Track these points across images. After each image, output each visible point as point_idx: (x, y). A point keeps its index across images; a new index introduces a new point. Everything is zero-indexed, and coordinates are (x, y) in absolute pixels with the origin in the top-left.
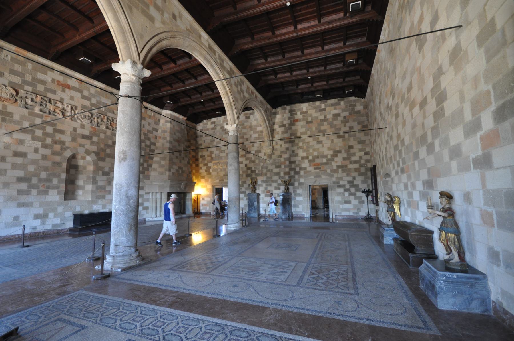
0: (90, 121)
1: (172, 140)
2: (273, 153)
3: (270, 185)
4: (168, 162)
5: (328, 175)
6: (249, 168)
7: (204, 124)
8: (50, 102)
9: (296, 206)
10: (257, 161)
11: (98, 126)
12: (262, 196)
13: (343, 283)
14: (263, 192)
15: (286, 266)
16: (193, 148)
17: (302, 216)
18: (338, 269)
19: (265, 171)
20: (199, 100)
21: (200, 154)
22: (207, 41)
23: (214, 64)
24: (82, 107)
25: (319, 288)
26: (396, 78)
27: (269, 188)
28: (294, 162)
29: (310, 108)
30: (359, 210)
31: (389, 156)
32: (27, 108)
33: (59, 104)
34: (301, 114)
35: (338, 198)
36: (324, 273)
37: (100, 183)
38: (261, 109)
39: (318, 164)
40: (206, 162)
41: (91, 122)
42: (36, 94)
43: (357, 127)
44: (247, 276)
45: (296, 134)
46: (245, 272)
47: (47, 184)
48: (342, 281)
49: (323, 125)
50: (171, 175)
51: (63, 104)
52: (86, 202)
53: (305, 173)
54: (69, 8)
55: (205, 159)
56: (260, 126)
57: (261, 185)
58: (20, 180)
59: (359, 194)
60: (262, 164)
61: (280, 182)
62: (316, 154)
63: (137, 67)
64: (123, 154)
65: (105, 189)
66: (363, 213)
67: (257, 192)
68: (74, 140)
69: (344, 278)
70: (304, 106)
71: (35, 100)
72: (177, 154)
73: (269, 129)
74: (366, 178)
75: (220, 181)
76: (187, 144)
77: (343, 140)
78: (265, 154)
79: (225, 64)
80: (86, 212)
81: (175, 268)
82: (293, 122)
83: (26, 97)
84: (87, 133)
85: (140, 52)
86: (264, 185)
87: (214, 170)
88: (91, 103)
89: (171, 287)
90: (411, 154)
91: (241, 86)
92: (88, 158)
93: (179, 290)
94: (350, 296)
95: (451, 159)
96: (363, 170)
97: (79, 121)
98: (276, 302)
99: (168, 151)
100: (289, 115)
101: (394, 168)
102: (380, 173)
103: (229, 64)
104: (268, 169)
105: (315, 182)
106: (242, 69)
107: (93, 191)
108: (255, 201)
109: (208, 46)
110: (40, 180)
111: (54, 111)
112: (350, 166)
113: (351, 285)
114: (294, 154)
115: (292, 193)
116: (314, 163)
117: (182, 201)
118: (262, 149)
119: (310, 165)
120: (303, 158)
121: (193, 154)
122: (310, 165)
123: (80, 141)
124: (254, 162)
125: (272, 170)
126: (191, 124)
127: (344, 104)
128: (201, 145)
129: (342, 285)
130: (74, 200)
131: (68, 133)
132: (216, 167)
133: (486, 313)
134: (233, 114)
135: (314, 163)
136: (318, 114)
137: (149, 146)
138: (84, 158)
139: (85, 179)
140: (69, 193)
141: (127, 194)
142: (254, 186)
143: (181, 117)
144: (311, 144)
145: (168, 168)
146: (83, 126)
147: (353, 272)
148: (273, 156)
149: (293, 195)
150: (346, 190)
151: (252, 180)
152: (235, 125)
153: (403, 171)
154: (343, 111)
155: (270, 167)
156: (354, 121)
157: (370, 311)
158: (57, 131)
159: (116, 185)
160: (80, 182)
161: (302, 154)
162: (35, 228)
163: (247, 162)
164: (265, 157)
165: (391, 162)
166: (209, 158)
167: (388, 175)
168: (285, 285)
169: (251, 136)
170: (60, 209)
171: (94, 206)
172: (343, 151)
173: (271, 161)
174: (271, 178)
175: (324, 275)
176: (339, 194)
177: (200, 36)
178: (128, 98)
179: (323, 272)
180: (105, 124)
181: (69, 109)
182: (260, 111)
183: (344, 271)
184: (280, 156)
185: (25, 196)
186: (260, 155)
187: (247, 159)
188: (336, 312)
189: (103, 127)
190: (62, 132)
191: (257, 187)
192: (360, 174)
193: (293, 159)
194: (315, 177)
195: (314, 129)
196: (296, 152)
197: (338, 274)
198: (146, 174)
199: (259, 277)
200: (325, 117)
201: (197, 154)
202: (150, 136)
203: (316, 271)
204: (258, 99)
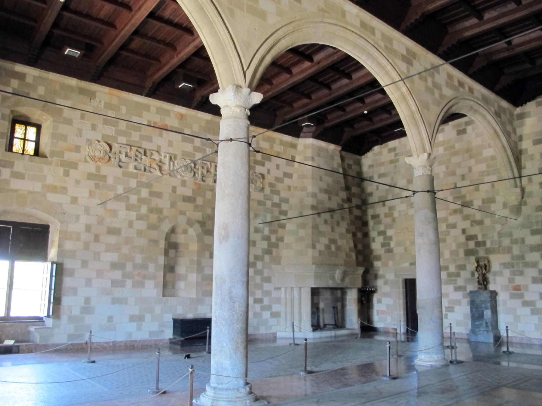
0: (193, 174)
1: (316, 190)
3: (521, 273)
4: (310, 231)
6: (469, 238)
7: (375, 155)
8: (145, 154)
10: (488, 222)
11: (203, 181)
16: (356, 201)
19: (506, 242)
20: (359, 112)
21: (370, 212)
22: (357, 16)
24: (183, 155)
27: (519, 280)
32: (120, 166)
33: (156, 156)
38: (485, 112)
40: (382, 228)
41: (194, 175)
42: (131, 146)
50: (317, 254)
51: (160, 154)
54: (163, 25)
55: (380, 222)
56: (490, 146)
57: (501, 274)
58: (114, 266)
60: (498, 227)
67: (492, 287)
68: (173, 205)
71: (129, 154)
72: (327, 216)
78: (505, 206)
83: (120, 152)
84: (189, 192)
85: (245, 69)
86: (507, 272)
87: (399, 244)
88: (194, 147)
91: (433, 76)
92: (191, 231)
97: (179, 176)
99: (311, 212)
103: (403, 42)
106: (431, 45)
107: (198, 284)
108: (486, 308)
109: (359, 25)
110: (135, 266)
111: (150, 167)
117: (339, 305)
121: (357, 212)
123: (182, 205)
124: (480, 223)
125: (523, 240)
126: (350, 158)
128: (371, 194)
130: (174, 296)
131: (166, 196)
134: (420, 133)
137: (277, 205)
138: (185, 232)
140: (168, 287)
141: (230, 293)
142: (484, 275)
143: (332, 147)
145: (310, 242)
146: (184, 183)
151: (478, 262)
152: (426, 155)
155: (518, 234)
159: (216, 278)
160: (181, 270)
162: (130, 334)
163: (466, 224)
164: (506, 212)
166: (388, 220)
169: (470, 169)
170: (158, 310)
171: (199, 307)
174: (522, 257)
177: (343, 13)
180: (213, 175)
181: (167, 160)
182: (484, 117)
185: (119, 289)
186: (493, 207)
187: (466, 218)
190: (159, 195)
191: (490, 276)
198: (274, 254)
201: (365, 212)
202: (280, 186)
204: (476, 94)
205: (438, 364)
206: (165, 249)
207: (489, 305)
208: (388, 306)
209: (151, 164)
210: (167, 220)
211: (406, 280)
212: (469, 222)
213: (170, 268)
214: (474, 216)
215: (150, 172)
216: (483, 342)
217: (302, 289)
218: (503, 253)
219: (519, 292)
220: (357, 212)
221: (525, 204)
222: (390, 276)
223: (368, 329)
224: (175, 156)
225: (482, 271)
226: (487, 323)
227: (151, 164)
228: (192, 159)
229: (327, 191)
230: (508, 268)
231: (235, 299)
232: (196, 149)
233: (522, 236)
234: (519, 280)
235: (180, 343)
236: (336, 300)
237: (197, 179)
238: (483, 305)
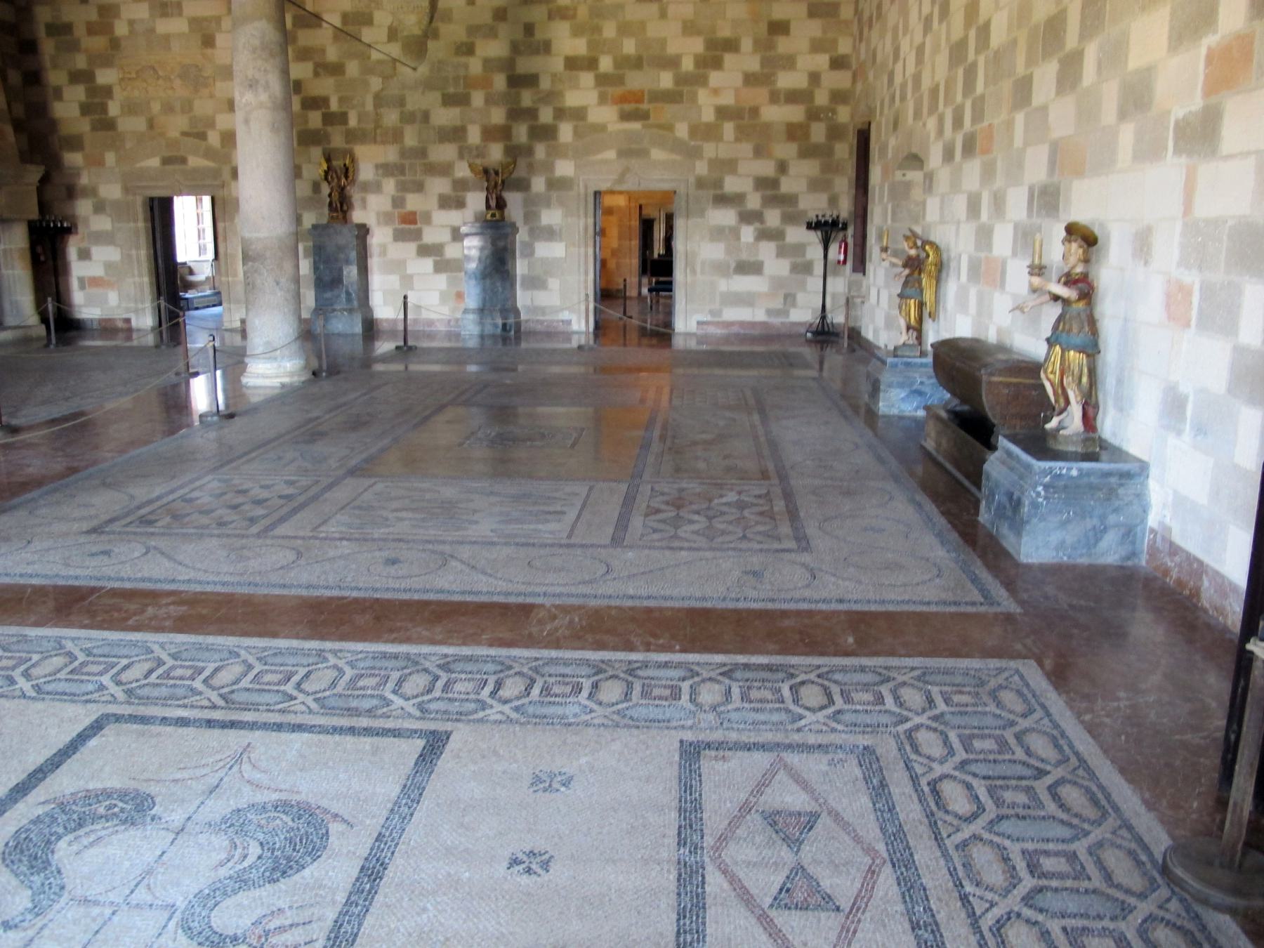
2: (430, 33)
3: (419, 187)
5: (678, 146)
6: (313, 103)
9: (535, 283)
10: (353, 69)
12: (380, 237)
13: (761, 528)
14: (386, 218)
15: (557, 495)
17: (561, 327)
18: (740, 493)
19: (391, 117)
25: (686, 545)
27: (413, 202)
28: (530, 80)
30: (790, 299)
31: (926, 83)
35: (712, 251)
36: (694, 507)
39: (637, 97)
40: (81, 62)
44: (422, 531)
48: (757, 523)
53: (576, 133)
55: (74, 47)
57: (377, 188)
59: (798, 234)
60: (376, 83)
66: (804, 314)
67: (358, 216)
69: (761, 514)
74: (830, 168)
75: (166, 161)
78: (393, 34)
81: (116, 527)
86: (390, 185)
87: (131, 109)
89: (143, 580)
90: (1006, 86)
93: (183, 587)
94: (787, 556)
95: (1123, 115)
96: (818, 133)
98: (558, 590)
101: (940, 132)
102: (883, 149)
104: (410, 107)
105: (621, 179)
108: (348, 262)
113: (785, 529)
115: (520, 224)
119: (603, 99)
120: (573, 64)
122: (603, 99)
124: (336, 69)
125: (426, 116)
129: (760, 533)
133: (1130, 563)
142: (343, 189)
147: (788, 496)
149: (522, 236)
150: (748, 217)
151: (328, 160)
153: (969, 148)
155: (416, 101)
157: (847, 583)
161: (567, 42)
164: (395, 50)
165: (933, 108)
166: (98, 43)
167: (915, 160)
168: (568, 546)
172: (747, 44)
173: (423, 69)
174: (422, 153)
175: (698, 513)
176: (718, 233)
179: (691, 503)
183: (760, 497)
184: (469, 50)
186: (367, 35)
188: (754, 594)
191: (355, 195)
192: (808, 152)
193: (525, 65)
194: (624, 153)
196: (539, 35)
197: (741, 506)
199: (470, 532)
203: (667, 503)
205: (296, 380)
207: (353, 255)
208: (108, 266)
211: (152, 199)
214: (323, 51)
216: (339, 335)
218: (383, 143)
219: (412, 227)
221: (436, 35)
222: (111, 191)
223: (63, 325)
225: (339, 179)
226: (348, 294)
230: (392, 175)
234: (413, 202)
238: (342, 256)
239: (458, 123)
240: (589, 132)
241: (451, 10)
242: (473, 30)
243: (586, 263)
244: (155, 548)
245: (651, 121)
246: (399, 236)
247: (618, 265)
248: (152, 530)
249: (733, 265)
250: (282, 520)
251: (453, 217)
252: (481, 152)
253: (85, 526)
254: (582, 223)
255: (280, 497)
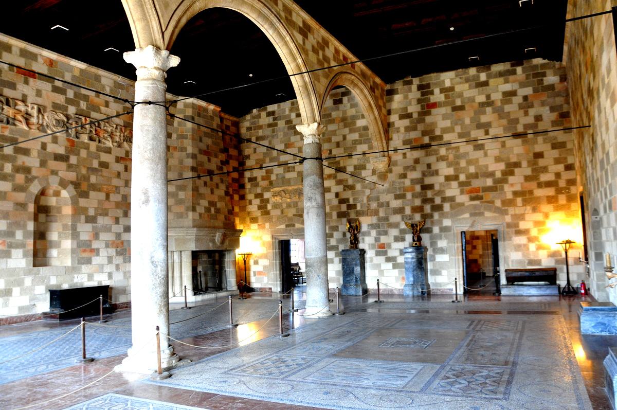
1: (196, 152)
3: (386, 233)
4: (190, 193)
6: (343, 201)
8: (8, 104)
9: (436, 272)
10: (358, 187)
11: (77, 137)
12: (370, 254)
13: (490, 388)
14: (372, 246)
16: (234, 163)
19: (374, 205)
21: (247, 174)
23: (275, 20)
24: (53, 107)
26: (594, 44)
27: (383, 239)
28: (431, 187)
29: (458, 80)
34: (441, 92)
37: (84, 237)
38: (362, 86)
40: (259, 191)
43: (549, 117)
45: (433, 131)
46: (341, 378)
47: (8, 240)
48: (491, 385)
49: (484, 113)
52: (68, 270)
53: (452, 207)
55: (257, 185)
56: (363, 117)
57: (368, 234)
60: (368, 192)
61: (403, 226)
62: (472, 169)
63: (160, 55)
64: (145, 194)
65: (90, 245)
67: (361, 246)
68: (43, 164)
69: (494, 381)
70: (447, 78)
72: (207, 179)
73: (380, 123)
75: (287, 226)
76: (222, 157)
77: (524, 142)
79: (294, 18)
80: (65, 286)
82: (427, 107)
84: (61, 150)
85: (164, 30)
86: (374, 233)
87: (276, 206)
88: (66, 98)
89: (233, 393)
91: (323, 50)
92: (65, 194)
100: (418, 95)
104: (381, 201)
105: (472, 225)
107: (73, 251)
108: (356, 265)
111: (14, 119)
112: (539, 192)
114: (430, 171)
116: (469, 188)
118: (368, 162)
119: (462, 193)
120: (448, 178)
121: (235, 175)
122: (462, 193)
123: (53, 164)
124: (352, 187)
125: (388, 204)
126: (229, 119)
127: (524, 72)
129: (489, 390)
131: (34, 153)
132: (278, 199)
134: (311, 104)
135: (469, 188)
136: (473, 92)
138: (57, 194)
139: (61, 230)
140: (39, 257)
143: (212, 107)
144: (462, 150)
145: (190, 204)
148: (389, 175)
151: (350, 224)
152: (316, 125)
154: (523, 85)
155: (384, 198)
156: (543, 104)
158: (18, 151)
160: (53, 236)
161: (445, 170)
163: (340, 188)
164: (374, 179)
165: (598, 189)
166: (264, 183)
169: (344, 137)
170: (28, 281)
172: (524, 164)
173: (386, 185)
174: (387, 219)
178: (148, 106)
180: (88, 132)
181: (35, 112)
182: (362, 91)
183: (498, 373)
184: (404, 176)
186: (364, 173)
187: (339, 182)
189: (85, 138)
190: (26, 152)
191: (360, 238)
193: (428, 181)
194: (472, 215)
195: (467, 121)
196: (433, 168)
197: (487, 377)
199: (364, 383)
200: (488, 97)
201: (242, 175)
203: (454, 375)
204: (357, 69)
206: (35, 213)
208: (265, 267)
209: (15, 116)
210: (36, 182)
212: (342, 187)
213: (40, 236)
214: (347, 180)
215: (14, 125)
216: (352, 296)
217: (183, 253)
218: (371, 216)
220: (235, 175)
221: (390, 171)
224: (45, 108)
225: (354, 231)
226: (356, 278)
227: (15, 116)
228: (65, 113)
229: (206, 152)
230: (375, 228)
231: (157, 263)
232: (69, 101)
233: (387, 200)
234: (383, 239)
235: (58, 316)
236: (213, 263)
237: (68, 135)
239: (401, 206)
240: (457, 207)
241: (397, 161)
242: (406, 168)
243: (459, 263)
244: (242, 381)
245: (484, 200)
246: (378, 254)
247: (483, 261)
248: (244, 374)
249: (527, 262)
250: (294, 373)
251: (401, 245)
252: (411, 218)
253: (223, 371)
254: (458, 245)
255: (297, 364)
